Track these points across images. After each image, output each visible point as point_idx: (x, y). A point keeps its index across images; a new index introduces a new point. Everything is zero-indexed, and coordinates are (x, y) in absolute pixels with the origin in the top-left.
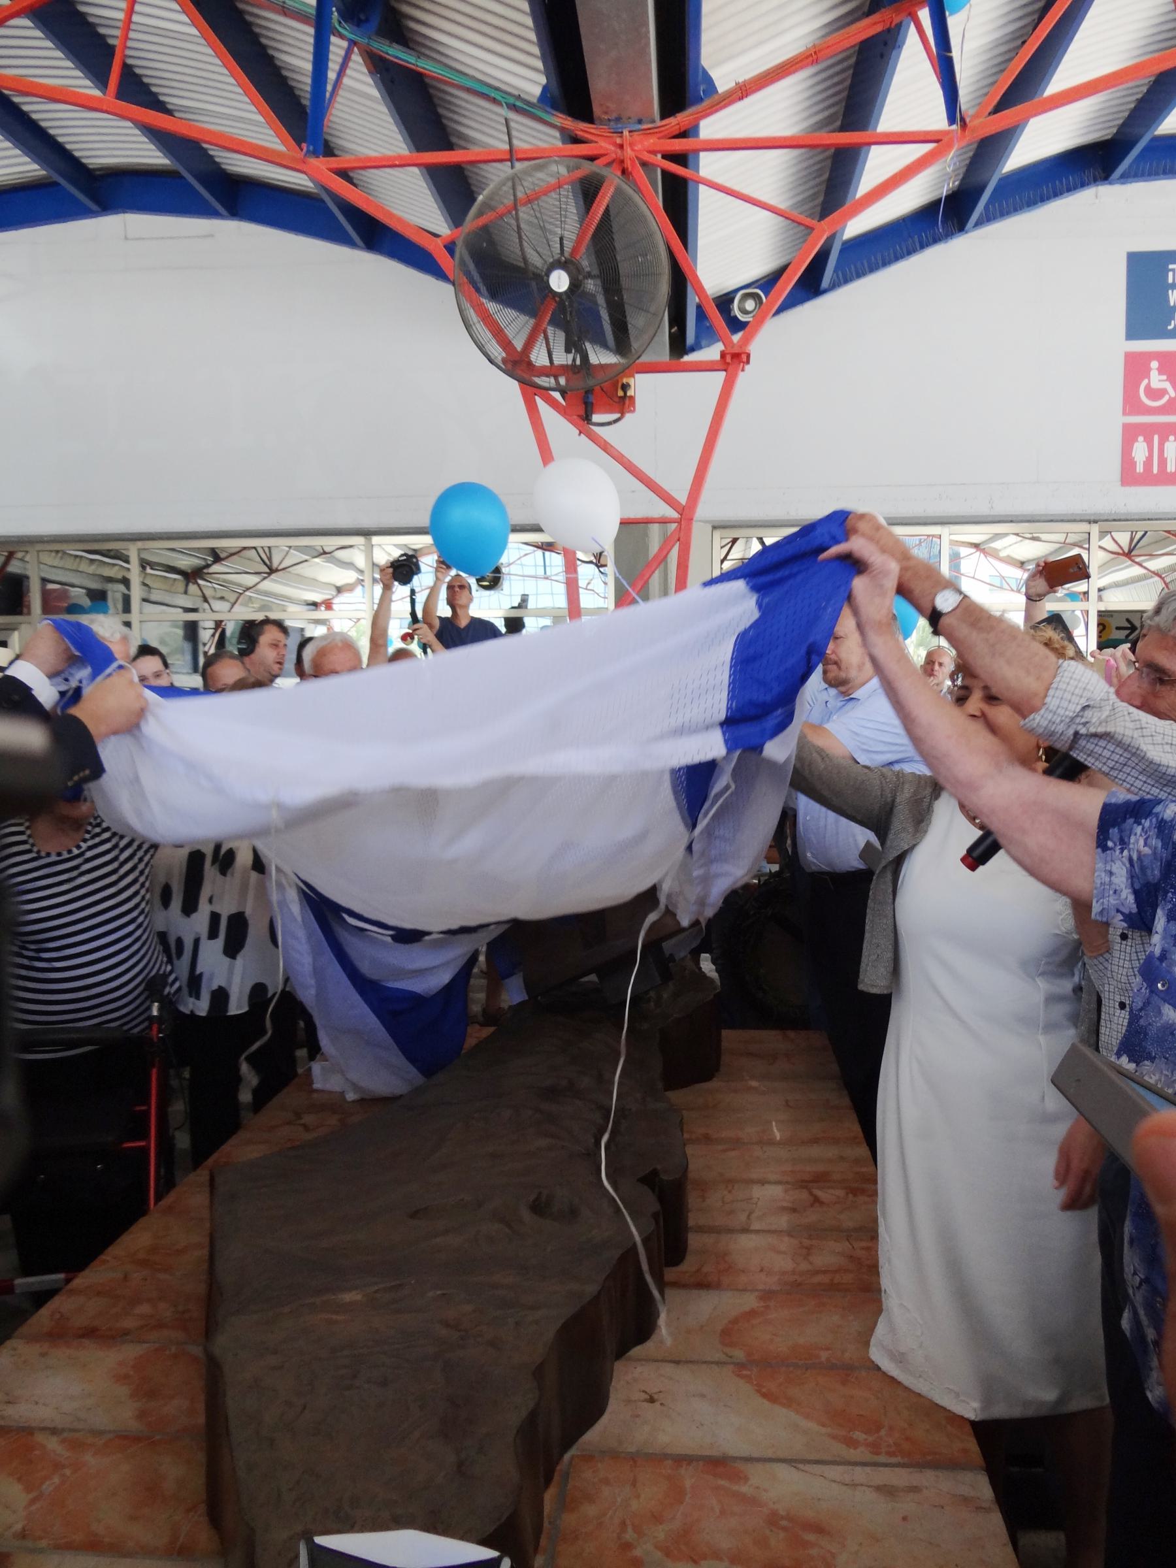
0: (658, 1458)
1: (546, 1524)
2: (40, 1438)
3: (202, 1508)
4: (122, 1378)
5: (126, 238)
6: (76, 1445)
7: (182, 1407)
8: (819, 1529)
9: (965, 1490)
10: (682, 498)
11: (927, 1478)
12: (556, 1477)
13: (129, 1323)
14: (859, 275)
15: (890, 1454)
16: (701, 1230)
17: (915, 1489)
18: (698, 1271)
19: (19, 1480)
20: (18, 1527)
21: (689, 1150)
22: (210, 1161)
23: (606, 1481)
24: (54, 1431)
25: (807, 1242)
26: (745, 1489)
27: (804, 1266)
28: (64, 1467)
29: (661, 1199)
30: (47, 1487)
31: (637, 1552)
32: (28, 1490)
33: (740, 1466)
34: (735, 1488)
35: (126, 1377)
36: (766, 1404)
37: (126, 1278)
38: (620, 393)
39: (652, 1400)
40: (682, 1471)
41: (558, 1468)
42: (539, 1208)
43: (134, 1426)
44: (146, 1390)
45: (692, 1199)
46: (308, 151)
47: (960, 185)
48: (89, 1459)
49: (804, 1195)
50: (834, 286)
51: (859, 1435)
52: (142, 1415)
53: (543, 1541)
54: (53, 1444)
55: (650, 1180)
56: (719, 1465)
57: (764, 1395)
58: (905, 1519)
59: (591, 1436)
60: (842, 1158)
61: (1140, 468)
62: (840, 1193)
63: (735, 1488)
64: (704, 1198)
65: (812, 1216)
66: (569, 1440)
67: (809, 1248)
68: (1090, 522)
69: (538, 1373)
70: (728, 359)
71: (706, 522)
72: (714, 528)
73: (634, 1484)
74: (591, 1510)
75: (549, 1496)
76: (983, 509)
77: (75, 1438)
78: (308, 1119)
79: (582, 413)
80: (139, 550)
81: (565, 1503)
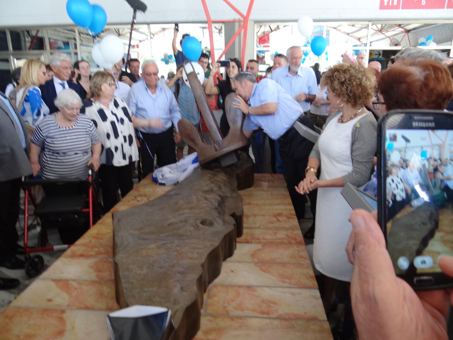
0: (233, 286)
1: (204, 302)
2: (71, 282)
3: (115, 299)
4: (92, 267)
6: (80, 284)
7: (108, 274)
8: (275, 303)
9: (313, 294)
12: (207, 291)
13: (92, 253)
15: (294, 285)
16: (247, 228)
17: (300, 294)
18: (246, 239)
20: (67, 304)
21: (244, 207)
22: (112, 210)
24: (74, 280)
25: (275, 231)
26: (256, 294)
27: (274, 237)
29: (236, 220)
30: (74, 294)
36: (262, 272)
37: (90, 241)
39: (232, 272)
42: (203, 223)
44: (98, 270)
45: (245, 220)
48: (84, 287)
49: (275, 219)
51: (286, 280)
52: (97, 276)
53: (204, 306)
54: (74, 284)
55: (233, 215)
56: (249, 287)
57: (261, 270)
58: (297, 301)
59: (217, 281)
60: (286, 209)
61: (386, 4)
62: (285, 218)
64: (248, 219)
65: (277, 225)
66: (210, 281)
67: (276, 233)
68: (369, 21)
69: (203, 265)
73: (227, 292)
74: (216, 299)
75: (205, 296)
76: (337, 17)
78: (139, 199)
81: (209, 297)
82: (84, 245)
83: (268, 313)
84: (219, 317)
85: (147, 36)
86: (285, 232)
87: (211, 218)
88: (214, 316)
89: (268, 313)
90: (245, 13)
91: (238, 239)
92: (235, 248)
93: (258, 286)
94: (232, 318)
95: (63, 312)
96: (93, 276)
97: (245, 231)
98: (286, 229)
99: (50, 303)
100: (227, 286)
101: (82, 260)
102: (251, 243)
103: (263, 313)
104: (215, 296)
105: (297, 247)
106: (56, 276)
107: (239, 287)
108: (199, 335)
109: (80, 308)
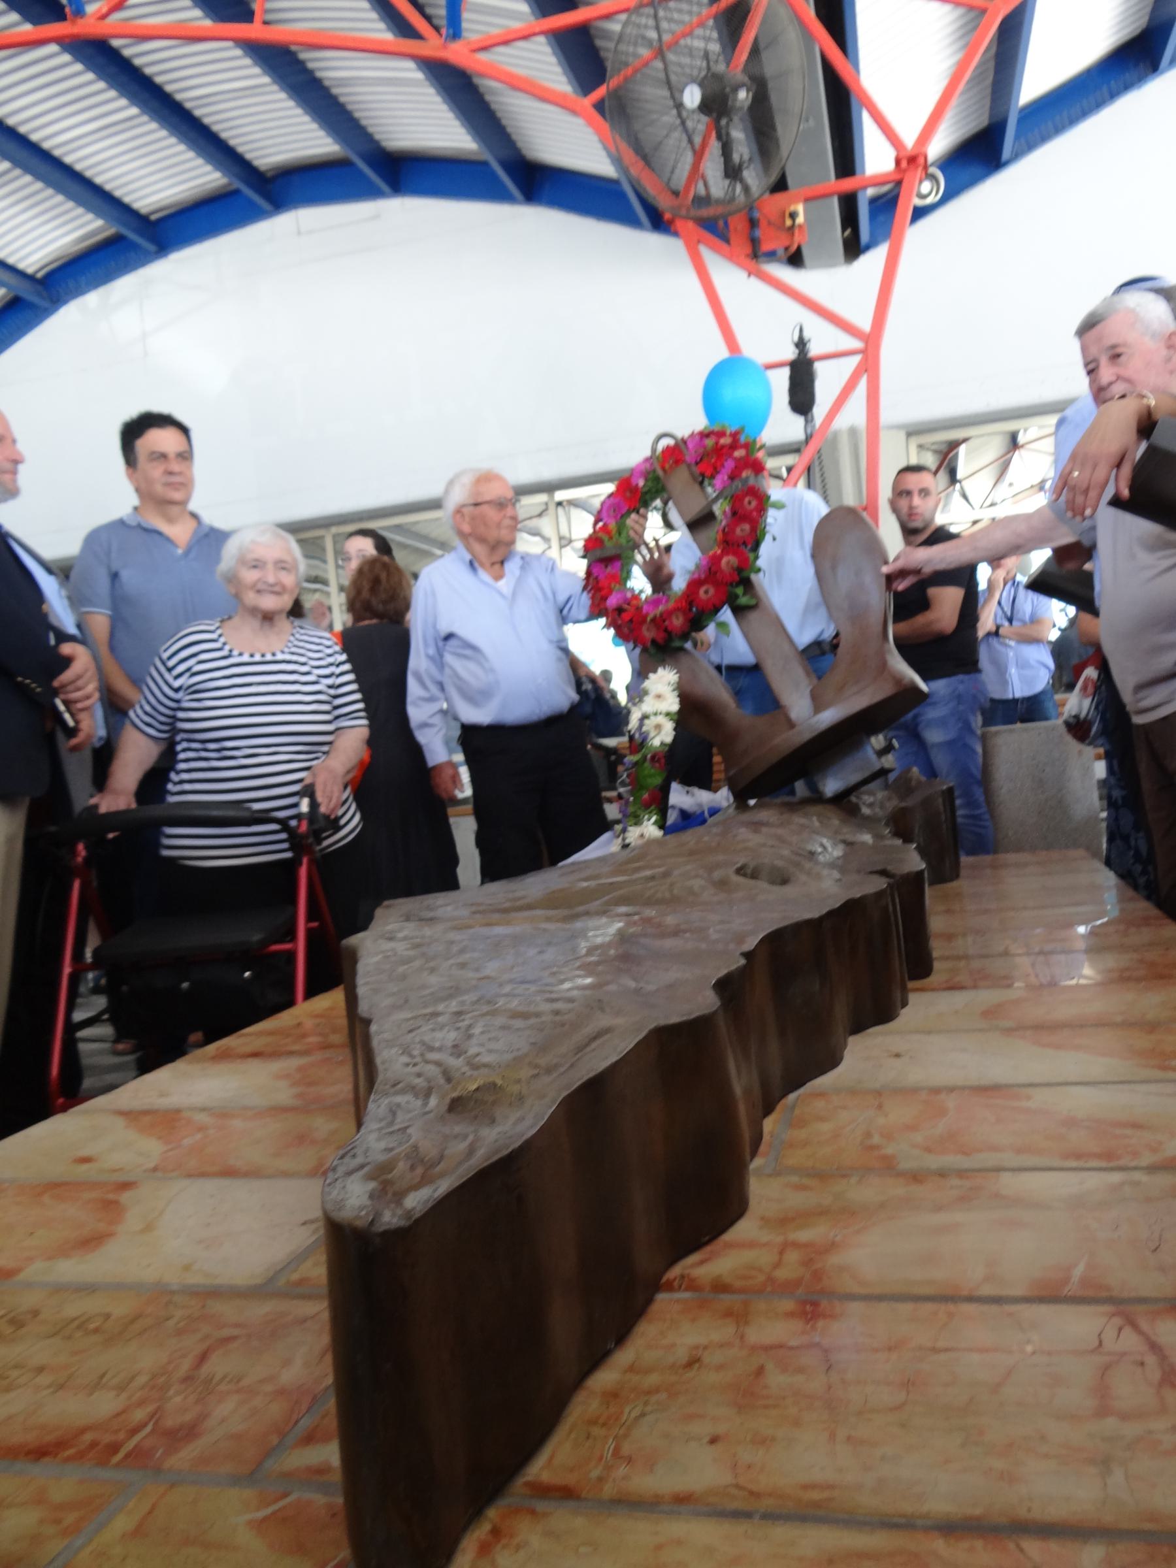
0: (908, 1092)
5: (299, 233)
8: (1136, 1126)
10: (866, 325)
12: (779, 1107)
13: (296, 1048)
14: (1044, 138)
19: (160, 1138)
20: (152, 1165)
24: (203, 1109)
30: (187, 1142)
31: (889, 1150)
38: (788, 222)
39: (897, 1055)
41: (783, 1101)
46: (447, 36)
47: (1150, 20)
48: (237, 1124)
50: (1017, 156)
70: (904, 164)
71: (898, 427)
73: (880, 1107)
74: (825, 1127)
77: (223, 1113)
79: (749, 250)
80: (334, 536)
82: (271, 1033)
83: (1109, 1155)
84: (844, 1176)
85: (546, 540)
87: (779, 863)
88: (821, 1176)
89: (1109, 1155)
92: (904, 1004)
93: (1031, 1085)
94: (916, 1177)
95: (126, 1186)
96: (284, 1095)
99: (85, 1167)
100: (878, 1093)
101: (254, 1065)
102: (975, 987)
103: (1078, 1156)
104: (822, 1119)
106: (137, 1104)
107: (936, 1091)
108: (744, 1229)
109: (203, 1175)
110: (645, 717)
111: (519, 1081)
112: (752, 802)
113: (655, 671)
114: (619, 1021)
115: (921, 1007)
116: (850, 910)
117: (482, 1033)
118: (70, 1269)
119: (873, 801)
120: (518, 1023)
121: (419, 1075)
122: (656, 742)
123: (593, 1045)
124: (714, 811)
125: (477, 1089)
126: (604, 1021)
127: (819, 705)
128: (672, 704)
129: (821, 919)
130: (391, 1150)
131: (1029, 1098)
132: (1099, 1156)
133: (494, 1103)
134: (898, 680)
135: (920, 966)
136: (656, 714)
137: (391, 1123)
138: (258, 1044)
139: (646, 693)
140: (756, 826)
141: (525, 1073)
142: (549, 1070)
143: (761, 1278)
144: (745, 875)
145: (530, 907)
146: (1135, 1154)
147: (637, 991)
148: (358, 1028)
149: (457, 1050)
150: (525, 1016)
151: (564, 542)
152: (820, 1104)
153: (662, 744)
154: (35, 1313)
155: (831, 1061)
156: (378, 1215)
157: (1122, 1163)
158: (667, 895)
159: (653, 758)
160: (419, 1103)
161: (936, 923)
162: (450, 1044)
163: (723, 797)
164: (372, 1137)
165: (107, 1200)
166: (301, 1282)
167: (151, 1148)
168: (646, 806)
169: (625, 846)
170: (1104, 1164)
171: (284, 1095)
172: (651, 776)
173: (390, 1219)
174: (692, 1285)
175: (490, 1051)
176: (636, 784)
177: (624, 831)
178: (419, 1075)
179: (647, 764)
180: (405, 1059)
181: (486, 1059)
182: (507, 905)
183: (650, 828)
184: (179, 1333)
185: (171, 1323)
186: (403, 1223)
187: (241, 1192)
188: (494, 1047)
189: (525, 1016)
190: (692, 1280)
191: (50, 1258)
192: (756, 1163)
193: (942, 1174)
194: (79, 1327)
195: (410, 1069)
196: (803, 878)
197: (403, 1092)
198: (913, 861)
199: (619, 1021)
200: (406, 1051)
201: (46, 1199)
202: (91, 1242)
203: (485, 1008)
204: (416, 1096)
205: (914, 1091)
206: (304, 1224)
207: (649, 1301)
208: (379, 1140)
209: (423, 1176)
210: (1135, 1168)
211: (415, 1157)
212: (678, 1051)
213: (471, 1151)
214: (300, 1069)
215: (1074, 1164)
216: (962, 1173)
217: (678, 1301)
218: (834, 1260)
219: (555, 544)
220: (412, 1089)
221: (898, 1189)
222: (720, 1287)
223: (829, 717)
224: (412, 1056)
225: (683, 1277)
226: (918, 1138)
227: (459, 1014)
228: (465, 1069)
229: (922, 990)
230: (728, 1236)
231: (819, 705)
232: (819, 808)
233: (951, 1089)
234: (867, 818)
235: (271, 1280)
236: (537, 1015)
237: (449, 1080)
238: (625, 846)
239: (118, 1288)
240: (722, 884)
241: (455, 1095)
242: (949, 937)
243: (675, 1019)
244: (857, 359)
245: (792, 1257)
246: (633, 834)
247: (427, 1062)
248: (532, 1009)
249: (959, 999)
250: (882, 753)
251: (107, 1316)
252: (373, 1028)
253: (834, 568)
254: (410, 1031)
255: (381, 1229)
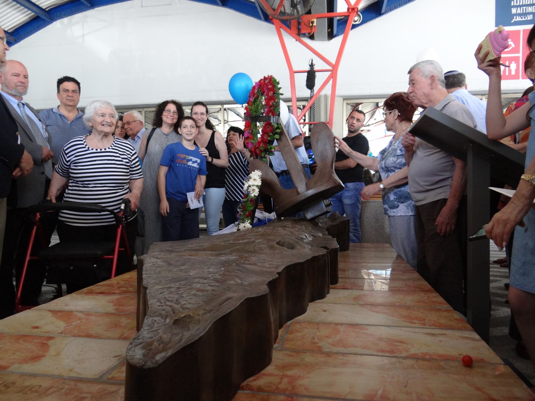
0: (328, 324)
2: (75, 313)
8: (402, 342)
11: (448, 332)
12: (284, 326)
23: (306, 328)
24: (81, 312)
28: (82, 319)
31: (320, 345)
32: (66, 323)
33: (363, 326)
34: (363, 331)
35: (113, 302)
39: (325, 311)
40: (339, 327)
43: (113, 311)
51: (414, 321)
53: (278, 340)
54: (80, 315)
58: (440, 341)
63: (363, 331)
69: (278, 273)
72: (344, 99)
73: (318, 329)
74: (299, 334)
77: (88, 314)
84: (305, 352)
86: (404, 283)
87: (292, 242)
88: (297, 352)
89: (392, 352)
90: (334, 62)
91: (331, 286)
92: (328, 293)
93: (368, 325)
94: (329, 354)
95: (51, 338)
96: (111, 309)
97: (340, 280)
98: (404, 280)
99: (36, 330)
101: (101, 297)
102: (351, 289)
103: (382, 351)
104: (298, 332)
105: (425, 294)
106: (57, 308)
107: (337, 324)
108: (270, 369)
109: (79, 336)
110: (249, 186)
111: (199, 315)
112: (282, 218)
113: (254, 171)
114: (235, 295)
115: (334, 295)
116: (314, 259)
117: (187, 296)
118: (28, 368)
119: (323, 222)
120: (200, 293)
121: (163, 310)
122: (253, 195)
123: (226, 303)
124: (270, 220)
125: (184, 317)
126: (230, 294)
127: (308, 188)
128: (259, 183)
129: (304, 263)
130: (152, 338)
131: (367, 329)
132: (389, 352)
133: (189, 322)
134: (335, 181)
135: (334, 280)
136: (253, 186)
137: (152, 328)
138: (103, 289)
139: (251, 178)
140: (284, 227)
141: (201, 312)
142: (210, 311)
143: (274, 387)
144: (279, 245)
145: (205, 250)
146: (401, 352)
147: (241, 284)
148: (141, 290)
149: (177, 302)
150: (202, 291)
151: (225, 122)
152: (298, 326)
153: (255, 196)
154: (14, 383)
155: (303, 311)
156: (146, 362)
157: (396, 355)
158: (253, 250)
159: (251, 200)
160: (163, 320)
161: (341, 265)
162: (175, 299)
163: (273, 215)
164: (145, 332)
165: (44, 342)
166: (113, 378)
167: (61, 325)
168: (247, 217)
169: (239, 230)
170: (390, 355)
171: (111, 309)
172: (249, 207)
173: (149, 365)
174: (250, 388)
175: (189, 303)
176: (244, 209)
177: (239, 224)
178: (163, 310)
179: (249, 202)
180: (158, 304)
181: (188, 306)
182: (197, 248)
183: (247, 225)
184: (66, 394)
185: (63, 390)
186: (156, 366)
187: (92, 343)
188: (190, 302)
189: (202, 291)
190: (250, 386)
191: (20, 363)
192: (275, 346)
193: (337, 353)
194: (29, 390)
195: (160, 308)
196: (299, 247)
197: (157, 316)
198: (335, 245)
199: (235, 295)
200: (159, 301)
201: (21, 341)
202: (36, 358)
203: (188, 287)
204: (162, 318)
205: (330, 323)
206: (115, 357)
207: (235, 394)
208: (148, 333)
209: (163, 348)
210: (401, 357)
211: (160, 341)
212: (253, 307)
213: (181, 340)
214: (117, 300)
215: (380, 354)
216: (343, 354)
217: (245, 393)
218: (300, 382)
219: (222, 122)
220: (160, 315)
221: (321, 358)
222: (260, 389)
223: (311, 192)
224: (161, 303)
225: (247, 385)
226: (330, 341)
227: (179, 288)
228: (180, 309)
229: (334, 288)
230: (263, 372)
231: (308, 188)
232: (305, 223)
233: (342, 324)
234: (320, 227)
235: (101, 377)
236: (207, 291)
237: (174, 313)
238: (239, 230)
239: (44, 376)
240: (272, 247)
241: (176, 318)
242: (344, 271)
243: (254, 296)
244: (330, 73)
245: (285, 380)
246: (242, 226)
247: (167, 305)
248: (205, 288)
249: (346, 293)
250: (327, 206)
251: (40, 386)
252: (148, 291)
253: (317, 142)
254: (161, 293)
255: (147, 367)
